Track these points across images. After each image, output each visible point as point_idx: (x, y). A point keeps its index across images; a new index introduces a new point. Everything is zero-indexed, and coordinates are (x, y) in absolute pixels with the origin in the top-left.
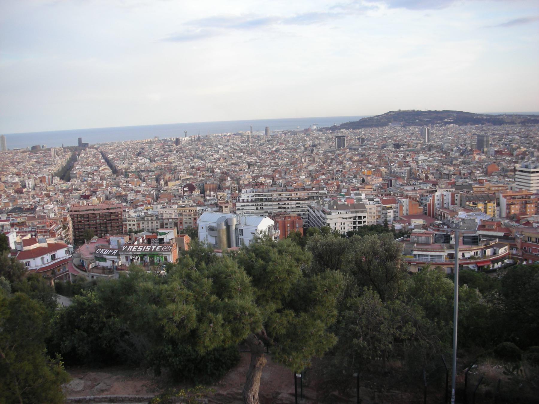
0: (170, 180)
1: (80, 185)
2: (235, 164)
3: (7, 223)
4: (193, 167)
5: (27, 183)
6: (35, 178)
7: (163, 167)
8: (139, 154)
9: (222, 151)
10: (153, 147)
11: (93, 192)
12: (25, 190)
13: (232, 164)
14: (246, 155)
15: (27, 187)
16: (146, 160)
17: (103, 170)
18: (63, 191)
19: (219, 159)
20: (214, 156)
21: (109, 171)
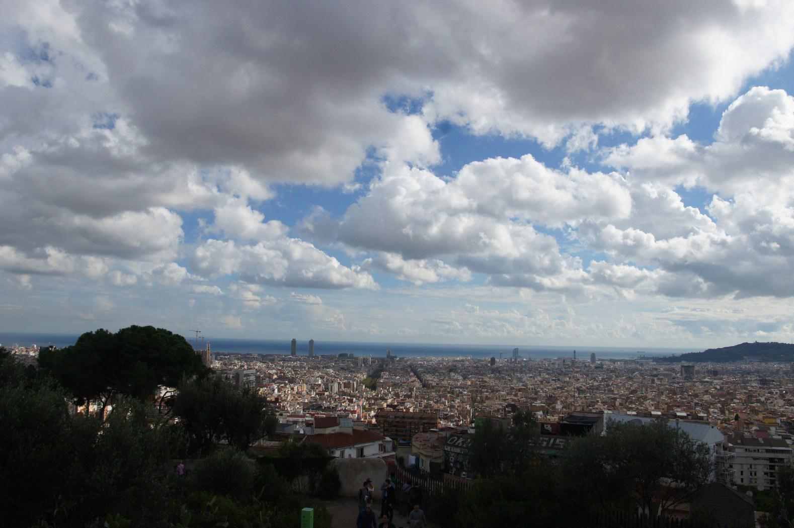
0: (487, 398)
1: (387, 395)
2: (562, 388)
3: (301, 419)
4: (512, 388)
5: (330, 386)
6: (339, 384)
7: (478, 385)
8: (451, 371)
9: (545, 374)
10: (466, 366)
11: (400, 403)
12: (326, 393)
13: (558, 388)
14: (572, 380)
15: (330, 390)
16: (459, 376)
17: (413, 382)
18: (368, 399)
19: (542, 382)
20: (536, 379)
21: (418, 384)
